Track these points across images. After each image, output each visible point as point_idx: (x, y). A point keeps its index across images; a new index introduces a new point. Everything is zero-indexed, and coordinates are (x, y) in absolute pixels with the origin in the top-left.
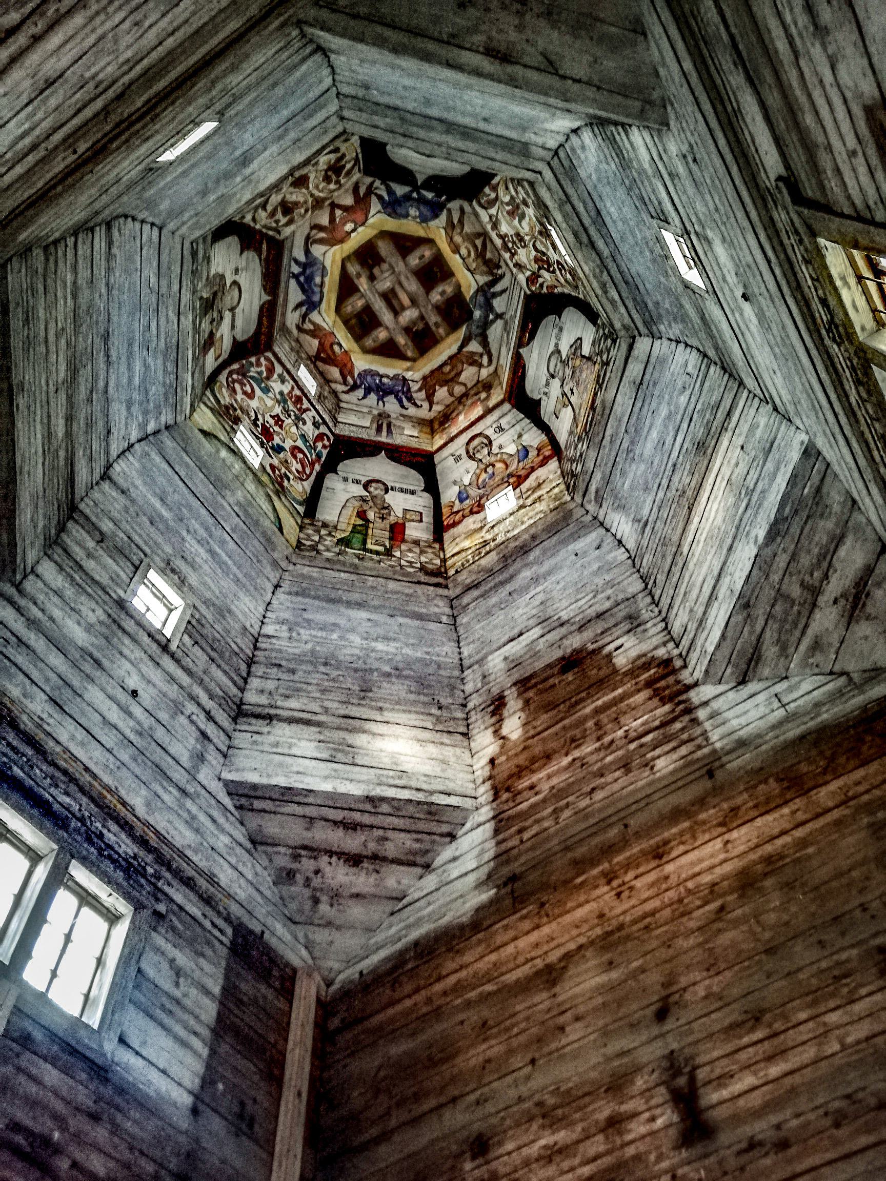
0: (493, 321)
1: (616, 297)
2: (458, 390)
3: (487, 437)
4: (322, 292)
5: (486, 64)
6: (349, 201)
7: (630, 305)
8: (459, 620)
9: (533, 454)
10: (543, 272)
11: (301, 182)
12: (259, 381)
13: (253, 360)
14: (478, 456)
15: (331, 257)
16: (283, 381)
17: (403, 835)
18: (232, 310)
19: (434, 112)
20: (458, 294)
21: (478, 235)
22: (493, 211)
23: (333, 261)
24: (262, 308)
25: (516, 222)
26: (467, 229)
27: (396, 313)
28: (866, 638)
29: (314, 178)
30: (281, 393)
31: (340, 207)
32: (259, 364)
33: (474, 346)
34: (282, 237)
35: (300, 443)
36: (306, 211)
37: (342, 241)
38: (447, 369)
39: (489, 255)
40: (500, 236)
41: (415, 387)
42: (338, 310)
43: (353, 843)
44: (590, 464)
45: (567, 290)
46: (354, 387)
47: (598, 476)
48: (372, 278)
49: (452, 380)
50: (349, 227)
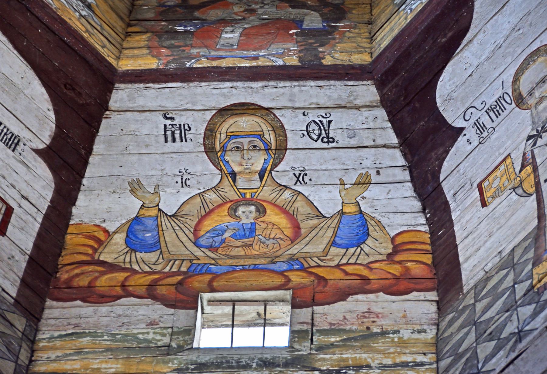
3: (280, 130)
9: (377, 247)
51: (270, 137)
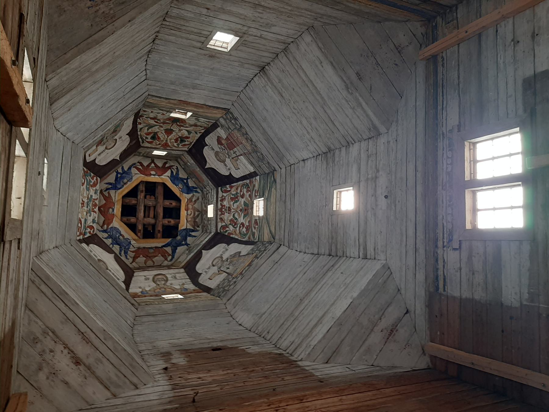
0: (183, 245)
1: (283, 226)
2: (150, 263)
3: (167, 277)
4: (123, 186)
5: (354, 77)
6: (160, 164)
7: (287, 231)
8: (136, 327)
10: (231, 227)
11: (169, 132)
12: (88, 184)
13: (92, 174)
14: (158, 283)
15: (137, 177)
16: (95, 193)
17: (111, 366)
18: (106, 148)
19: (264, 125)
20: (176, 227)
21: (198, 211)
22: (225, 195)
23: (137, 179)
24: (114, 160)
25: (232, 203)
26: (196, 206)
27: (144, 217)
28: (392, 350)
29: (173, 136)
30: (91, 196)
31: (155, 164)
32: (93, 178)
33: (169, 249)
34: (142, 145)
35: (83, 220)
36: (159, 144)
37: (146, 175)
38: (152, 251)
39: (197, 220)
40: (221, 204)
41: (132, 249)
42: (123, 197)
43: (82, 350)
44: (238, 287)
45: (236, 237)
46: (105, 231)
47: (240, 293)
48: (145, 197)
49: (150, 257)
50: (153, 172)
51: (165, 278)
